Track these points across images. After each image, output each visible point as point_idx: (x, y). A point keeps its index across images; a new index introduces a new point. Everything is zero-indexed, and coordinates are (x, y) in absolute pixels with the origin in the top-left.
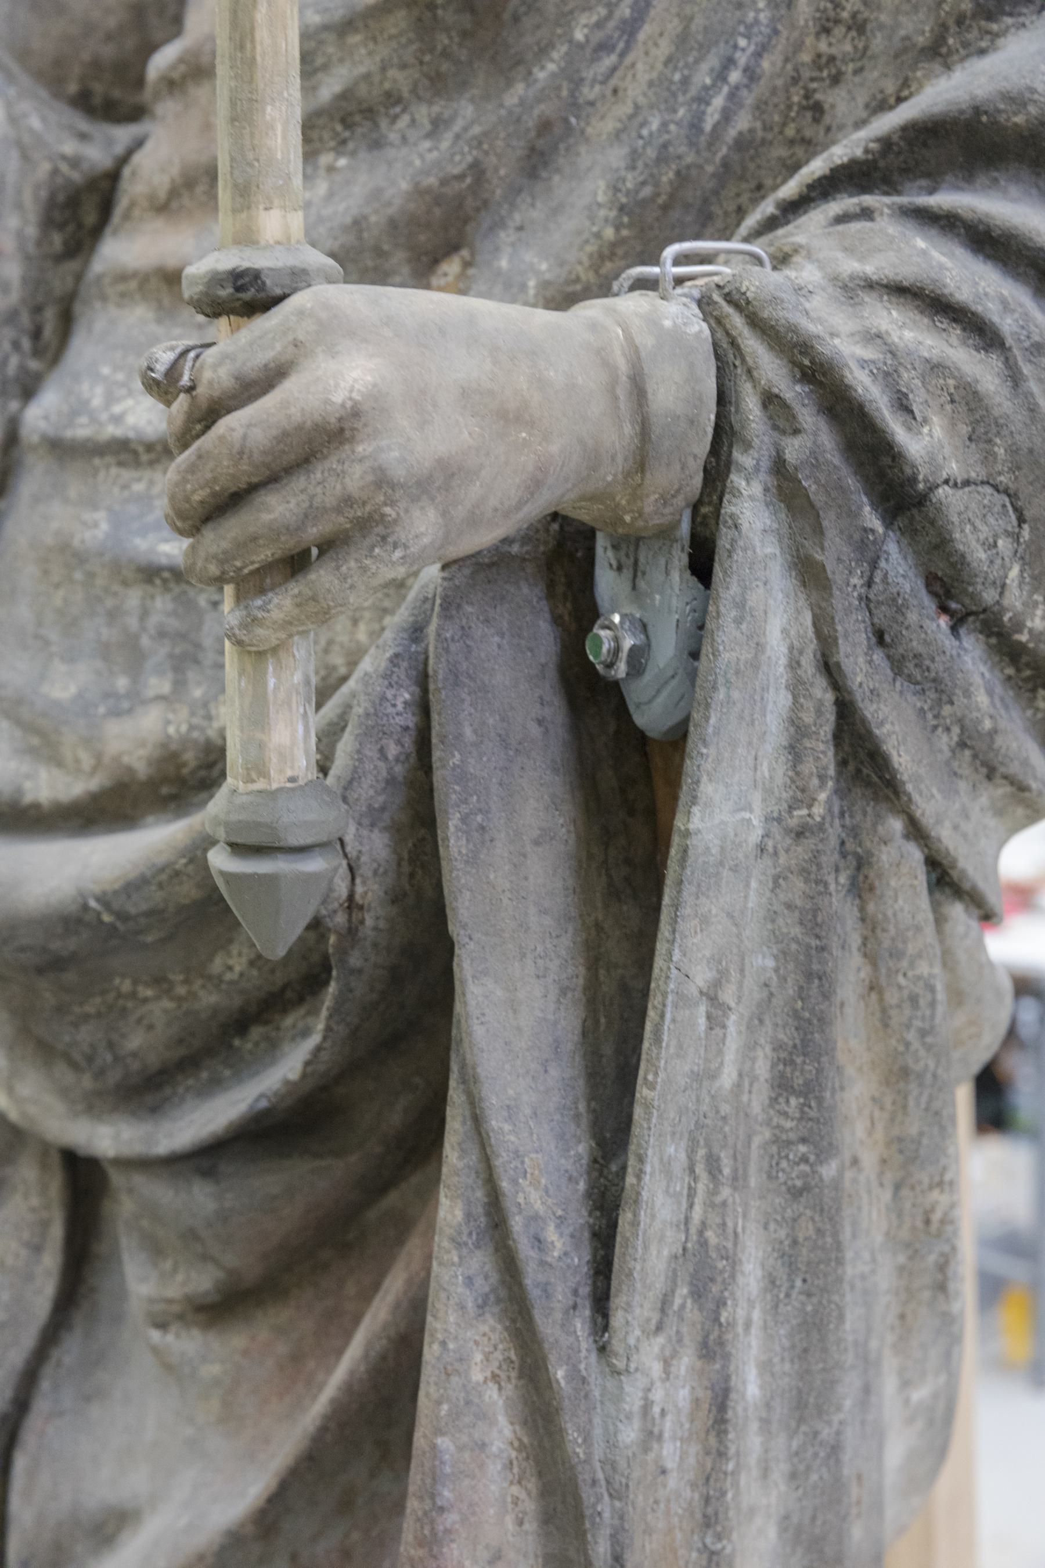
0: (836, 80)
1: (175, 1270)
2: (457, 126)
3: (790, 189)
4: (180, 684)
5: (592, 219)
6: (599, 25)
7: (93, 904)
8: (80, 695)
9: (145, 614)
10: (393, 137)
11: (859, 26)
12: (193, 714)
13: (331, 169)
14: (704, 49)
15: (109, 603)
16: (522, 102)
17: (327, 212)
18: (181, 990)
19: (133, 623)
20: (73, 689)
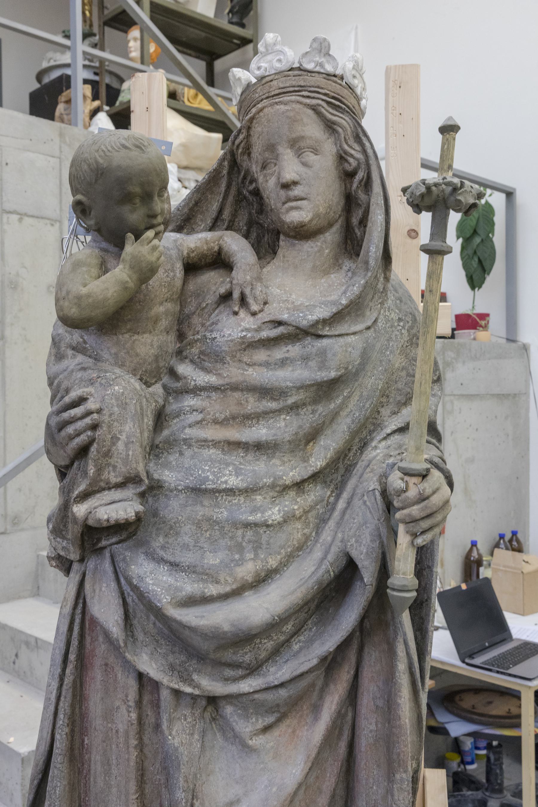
0: (383, 406)
1: (257, 720)
2: (319, 412)
3: (389, 431)
4: (256, 555)
5: (344, 434)
6: (349, 392)
7: (276, 618)
8: (221, 562)
9: (243, 536)
10: (302, 413)
11: (388, 397)
12: (262, 562)
13: (284, 419)
14: (367, 400)
15: (230, 534)
16: (334, 408)
17: (287, 430)
18: (275, 638)
19: (240, 539)
20: (218, 560)
